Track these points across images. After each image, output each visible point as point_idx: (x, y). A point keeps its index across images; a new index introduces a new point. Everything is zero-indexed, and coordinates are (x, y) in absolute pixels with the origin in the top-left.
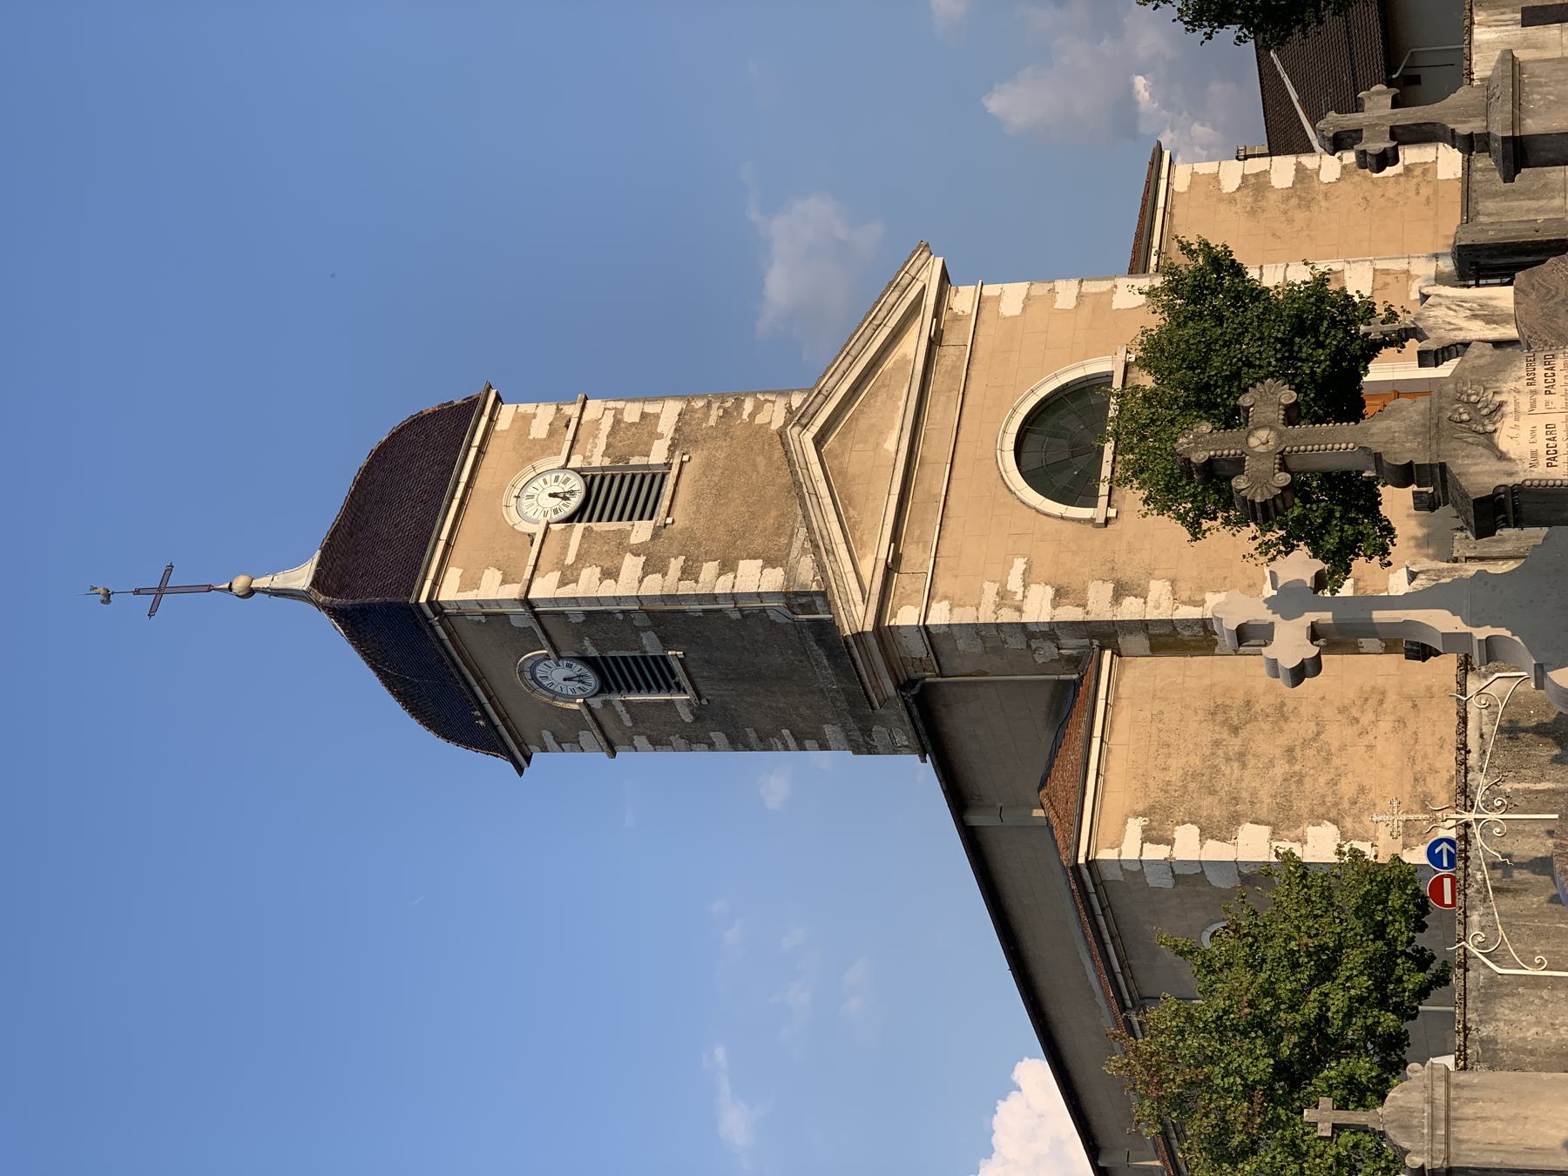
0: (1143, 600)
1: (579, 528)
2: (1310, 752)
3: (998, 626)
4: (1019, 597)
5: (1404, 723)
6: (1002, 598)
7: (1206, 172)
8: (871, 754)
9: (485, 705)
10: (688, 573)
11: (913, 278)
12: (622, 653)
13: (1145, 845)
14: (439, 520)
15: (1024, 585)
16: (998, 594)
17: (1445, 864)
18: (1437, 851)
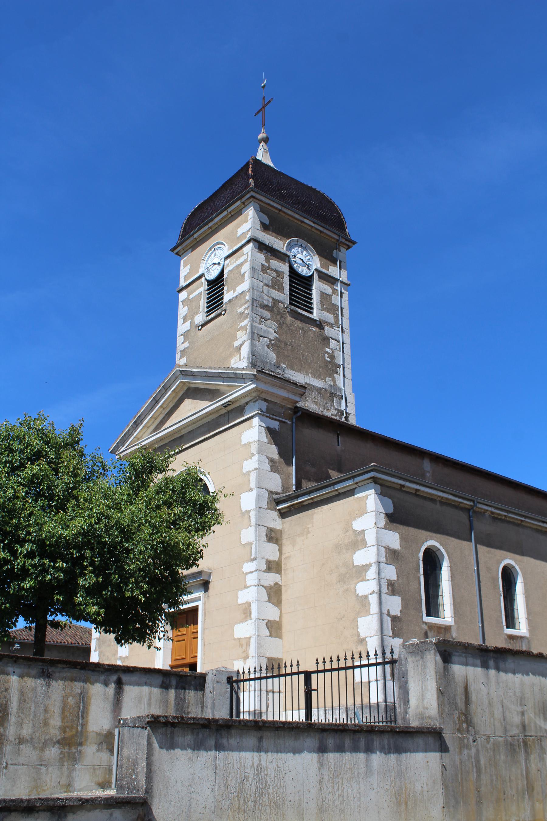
7: (368, 505)
14: (196, 229)
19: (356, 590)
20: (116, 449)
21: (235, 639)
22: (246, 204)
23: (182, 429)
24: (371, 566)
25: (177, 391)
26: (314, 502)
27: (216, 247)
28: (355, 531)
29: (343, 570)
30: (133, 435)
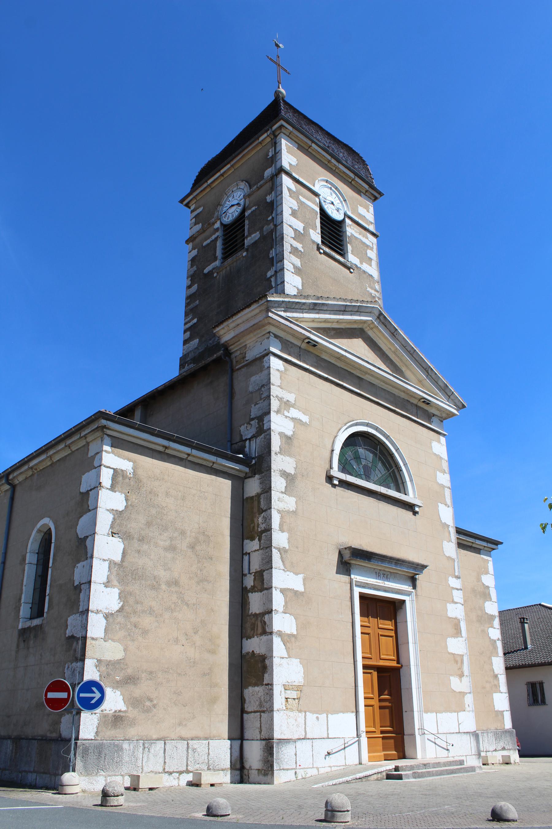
0: (284, 491)
1: (318, 210)
2: (174, 598)
3: (269, 397)
4: (286, 413)
5: (193, 666)
6: (285, 403)
8: (180, 366)
9: (219, 172)
10: (294, 251)
11: (449, 397)
12: (246, 227)
13: (112, 470)
15: (293, 418)
16: (288, 401)
17: (82, 695)
18: (94, 689)
20: (276, 305)
21: (449, 653)
22: (367, 194)
23: (369, 374)
27: (333, 188)
30: (302, 313)
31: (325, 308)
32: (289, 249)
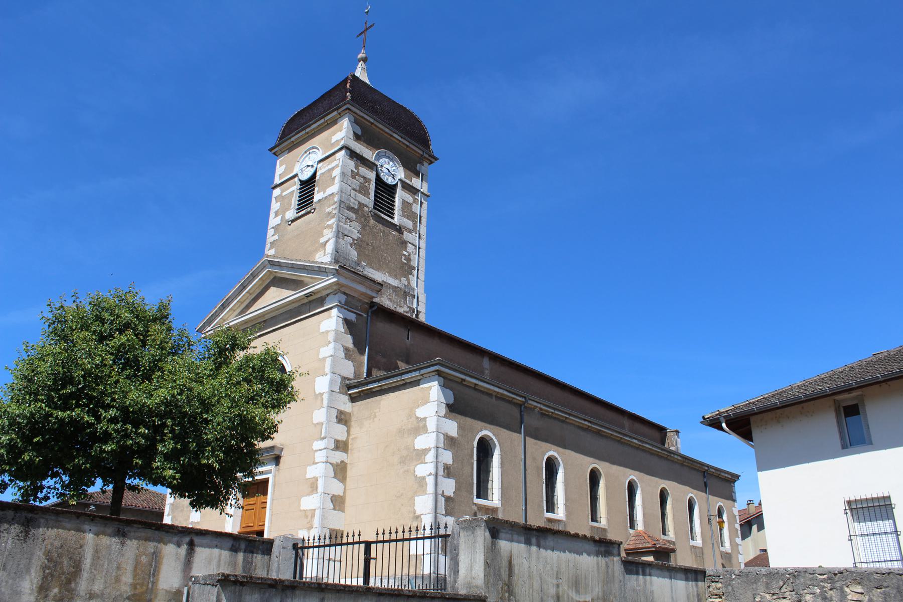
14: (294, 133)
19: (415, 472)
21: (301, 511)
22: (342, 115)
23: (266, 314)
24: (430, 450)
25: (264, 279)
26: (382, 390)
27: (311, 151)
28: (418, 418)
29: (405, 453)
31: (230, 300)
32: (372, 183)
